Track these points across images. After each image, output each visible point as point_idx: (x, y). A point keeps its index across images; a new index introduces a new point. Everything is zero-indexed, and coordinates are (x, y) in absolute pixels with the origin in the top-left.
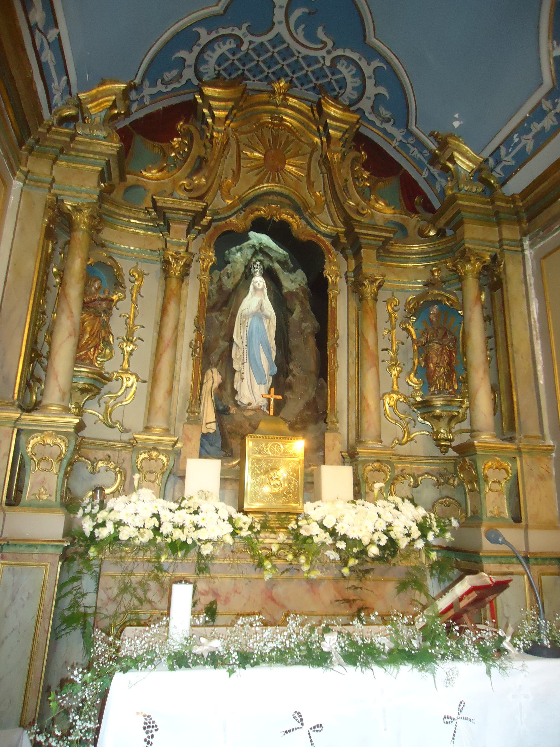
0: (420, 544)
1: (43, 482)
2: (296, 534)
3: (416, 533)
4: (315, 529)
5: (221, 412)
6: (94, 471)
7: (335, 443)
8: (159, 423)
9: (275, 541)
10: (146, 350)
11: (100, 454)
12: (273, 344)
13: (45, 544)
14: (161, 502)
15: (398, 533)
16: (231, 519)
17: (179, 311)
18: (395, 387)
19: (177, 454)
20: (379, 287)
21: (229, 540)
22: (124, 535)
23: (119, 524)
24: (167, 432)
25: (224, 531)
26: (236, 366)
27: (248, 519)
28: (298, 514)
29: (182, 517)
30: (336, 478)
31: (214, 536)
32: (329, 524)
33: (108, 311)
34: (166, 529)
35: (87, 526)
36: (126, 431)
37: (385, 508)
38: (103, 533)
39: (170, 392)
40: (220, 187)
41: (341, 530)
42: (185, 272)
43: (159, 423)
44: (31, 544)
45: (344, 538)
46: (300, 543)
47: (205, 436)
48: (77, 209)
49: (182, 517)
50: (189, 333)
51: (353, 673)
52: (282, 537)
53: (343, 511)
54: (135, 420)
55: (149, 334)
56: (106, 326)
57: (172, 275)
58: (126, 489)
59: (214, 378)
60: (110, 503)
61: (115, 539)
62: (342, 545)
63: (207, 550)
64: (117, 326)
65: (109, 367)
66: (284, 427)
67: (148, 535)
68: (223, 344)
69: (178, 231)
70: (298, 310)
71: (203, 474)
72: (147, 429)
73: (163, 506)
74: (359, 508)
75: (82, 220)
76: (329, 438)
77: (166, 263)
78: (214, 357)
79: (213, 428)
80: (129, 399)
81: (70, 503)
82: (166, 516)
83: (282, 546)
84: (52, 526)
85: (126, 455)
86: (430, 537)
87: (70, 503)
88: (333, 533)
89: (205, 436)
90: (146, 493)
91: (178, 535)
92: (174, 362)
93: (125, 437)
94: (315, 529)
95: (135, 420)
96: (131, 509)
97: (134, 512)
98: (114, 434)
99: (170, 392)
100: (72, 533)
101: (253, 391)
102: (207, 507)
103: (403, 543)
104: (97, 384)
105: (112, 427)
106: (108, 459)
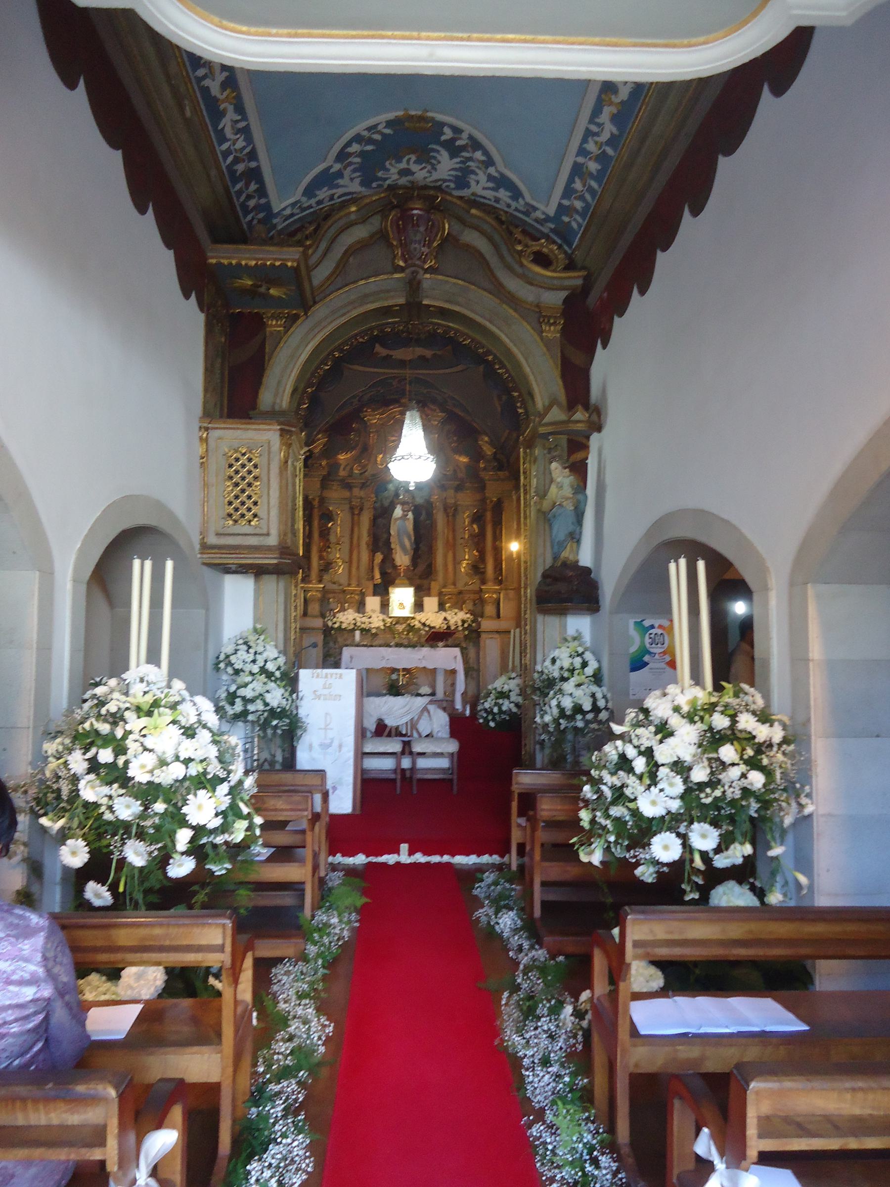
0: (460, 628)
1: (314, 608)
2: (409, 625)
3: (460, 623)
4: (417, 623)
5: (383, 574)
6: (329, 603)
7: (435, 586)
8: (354, 582)
9: (400, 628)
10: (346, 547)
11: (331, 595)
12: (412, 533)
13: (318, 629)
14: (357, 614)
15: (452, 622)
16: (383, 620)
17: (359, 528)
18: (467, 557)
19: (363, 595)
20: (456, 510)
21: (382, 627)
22: (343, 626)
23: (341, 622)
24: (358, 586)
25: (381, 624)
26: (393, 546)
27: (390, 620)
28: (413, 618)
29: (364, 619)
30: (431, 603)
31: (377, 625)
32: (423, 621)
33: (328, 534)
34: (358, 624)
35: (330, 624)
36: (340, 585)
37: (449, 615)
38: (336, 626)
39: (358, 568)
40: (376, 460)
41: (428, 623)
42: (361, 509)
43: (354, 582)
44: (313, 629)
45: (429, 626)
46: (411, 628)
47: (375, 585)
48: (314, 499)
49: (364, 619)
50: (365, 538)
51: (397, 649)
52: (404, 626)
53: (433, 616)
54: (344, 580)
55: (346, 540)
56: (328, 540)
57: (355, 511)
58: (343, 610)
59: (379, 557)
60: (337, 615)
61: (340, 628)
62: (427, 629)
63: (374, 631)
64: (332, 538)
65: (331, 557)
66: (406, 582)
67: (352, 627)
68: (385, 536)
69: (356, 492)
70: (424, 513)
71: (373, 603)
72: (349, 585)
73: (357, 616)
74: (438, 614)
75: (316, 503)
76: (433, 584)
77: (352, 508)
78: (381, 544)
79: (379, 581)
80: (340, 571)
81: (323, 616)
82: (358, 619)
83: (404, 630)
84: (318, 623)
85: (341, 596)
86: (466, 625)
87: (323, 616)
88: (424, 624)
89: (375, 585)
90: (350, 611)
91: (363, 626)
92: (359, 553)
93: (341, 587)
94: (417, 623)
95: (344, 580)
96: (345, 617)
97: (347, 618)
98: (335, 587)
99: (358, 568)
100: (325, 625)
101: (402, 559)
102: (374, 616)
103: (453, 628)
104: (327, 567)
105: (334, 583)
106: (334, 598)
